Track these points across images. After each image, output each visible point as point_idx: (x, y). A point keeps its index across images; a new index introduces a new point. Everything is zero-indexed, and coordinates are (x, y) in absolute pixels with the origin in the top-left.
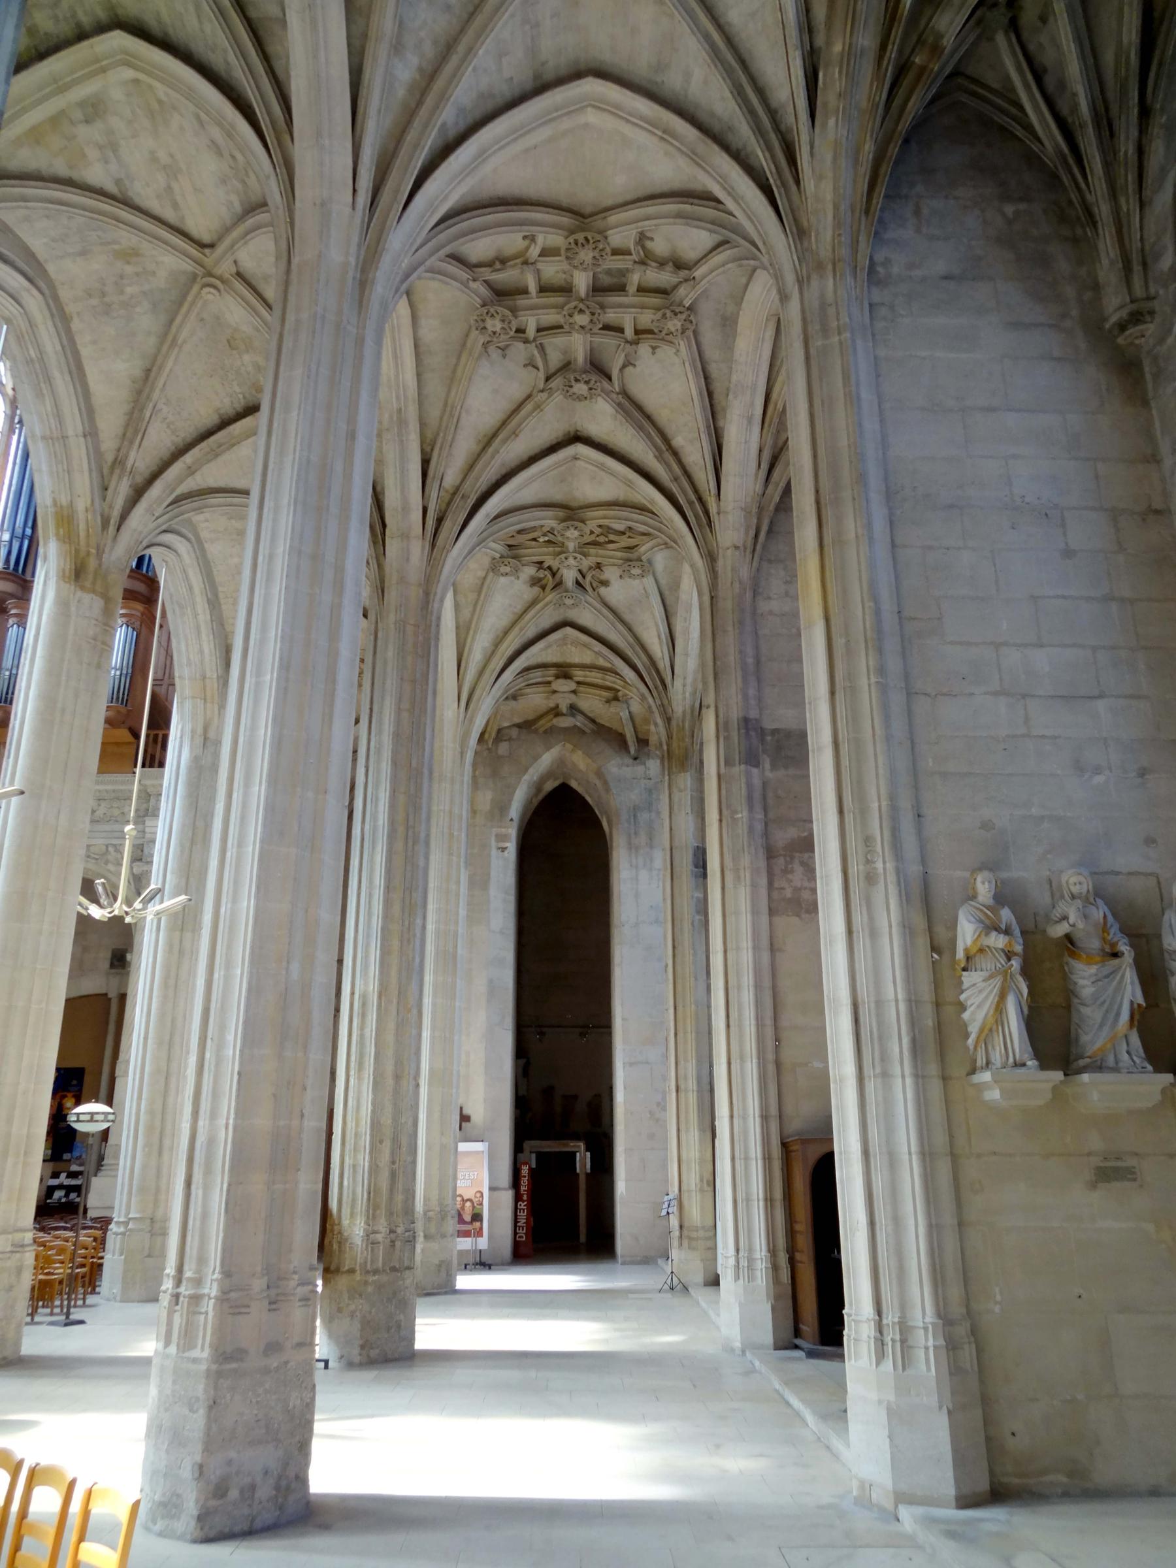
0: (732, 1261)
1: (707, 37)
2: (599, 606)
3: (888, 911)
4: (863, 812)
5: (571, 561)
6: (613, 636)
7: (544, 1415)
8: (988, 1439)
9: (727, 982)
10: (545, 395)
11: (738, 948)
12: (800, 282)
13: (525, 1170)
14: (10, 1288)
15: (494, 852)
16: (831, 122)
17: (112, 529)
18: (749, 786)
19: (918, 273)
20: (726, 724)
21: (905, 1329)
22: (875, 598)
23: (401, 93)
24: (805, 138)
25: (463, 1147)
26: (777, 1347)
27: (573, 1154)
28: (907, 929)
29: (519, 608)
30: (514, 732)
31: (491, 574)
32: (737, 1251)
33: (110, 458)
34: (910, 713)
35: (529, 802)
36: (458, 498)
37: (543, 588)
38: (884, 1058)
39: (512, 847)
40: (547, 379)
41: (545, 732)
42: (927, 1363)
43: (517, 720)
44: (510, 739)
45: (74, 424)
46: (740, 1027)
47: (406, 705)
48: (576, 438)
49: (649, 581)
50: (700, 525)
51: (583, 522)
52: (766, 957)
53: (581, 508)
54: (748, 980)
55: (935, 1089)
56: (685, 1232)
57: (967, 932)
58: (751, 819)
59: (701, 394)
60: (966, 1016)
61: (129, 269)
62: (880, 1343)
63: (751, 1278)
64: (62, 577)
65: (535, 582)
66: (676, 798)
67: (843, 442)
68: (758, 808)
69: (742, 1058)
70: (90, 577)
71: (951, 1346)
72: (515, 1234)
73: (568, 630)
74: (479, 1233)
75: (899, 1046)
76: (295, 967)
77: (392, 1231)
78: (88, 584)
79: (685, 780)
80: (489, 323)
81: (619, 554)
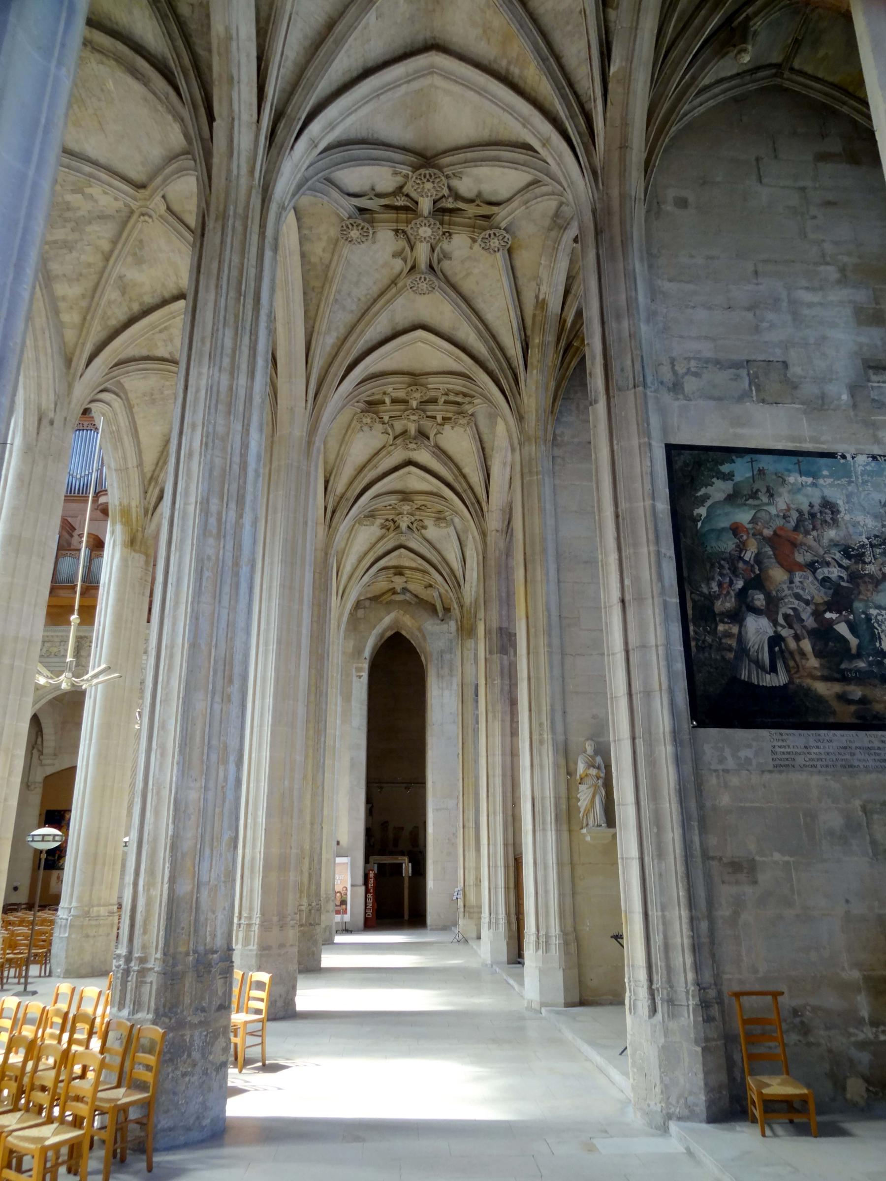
0: (487, 920)
1: (476, 327)
2: (420, 540)
3: (548, 756)
4: (539, 712)
5: (405, 519)
6: (428, 555)
7: (392, 988)
8: (580, 981)
9: (487, 772)
10: (393, 447)
11: (494, 755)
12: (520, 444)
13: (372, 874)
14: (108, 935)
15: (355, 679)
16: (535, 372)
17: (149, 515)
18: (501, 664)
19: (576, 440)
20: (490, 630)
21: (547, 936)
22: (548, 610)
23: (328, 349)
24: (523, 378)
26: (509, 963)
27: (400, 865)
28: (556, 765)
29: (374, 540)
30: (367, 603)
31: (357, 525)
32: (490, 914)
33: (148, 476)
34: (563, 664)
35: (376, 645)
36: (344, 500)
37: (388, 529)
38: (544, 822)
39: (365, 675)
40: (395, 438)
41: (387, 603)
42: (555, 950)
43: (369, 596)
44: (364, 608)
45: (132, 462)
46: (494, 797)
47: (315, 619)
48: (410, 463)
49: (451, 530)
50: (477, 516)
51: (413, 501)
52: (508, 759)
53: (411, 493)
54: (498, 771)
55: (565, 835)
56: (467, 909)
57: (581, 768)
58: (502, 684)
59: (478, 451)
60: (579, 804)
61: (168, 383)
62: (538, 943)
63: (497, 928)
64: (124, 545)
65: (383, 527)
66: (465, 655)
67: (537, 531)
68: (506, 677)
69: (495, 813)
70: (138, 544)
71: (566, 943)
72: (366, 913)
73: (402, 550)
74: (345, 912)
75: (550, 818)
76: (286, 783)
77: (310, 905)
78: (137, 548)
79: (470, 643)
80: (365, 420)
81: (433, 515)
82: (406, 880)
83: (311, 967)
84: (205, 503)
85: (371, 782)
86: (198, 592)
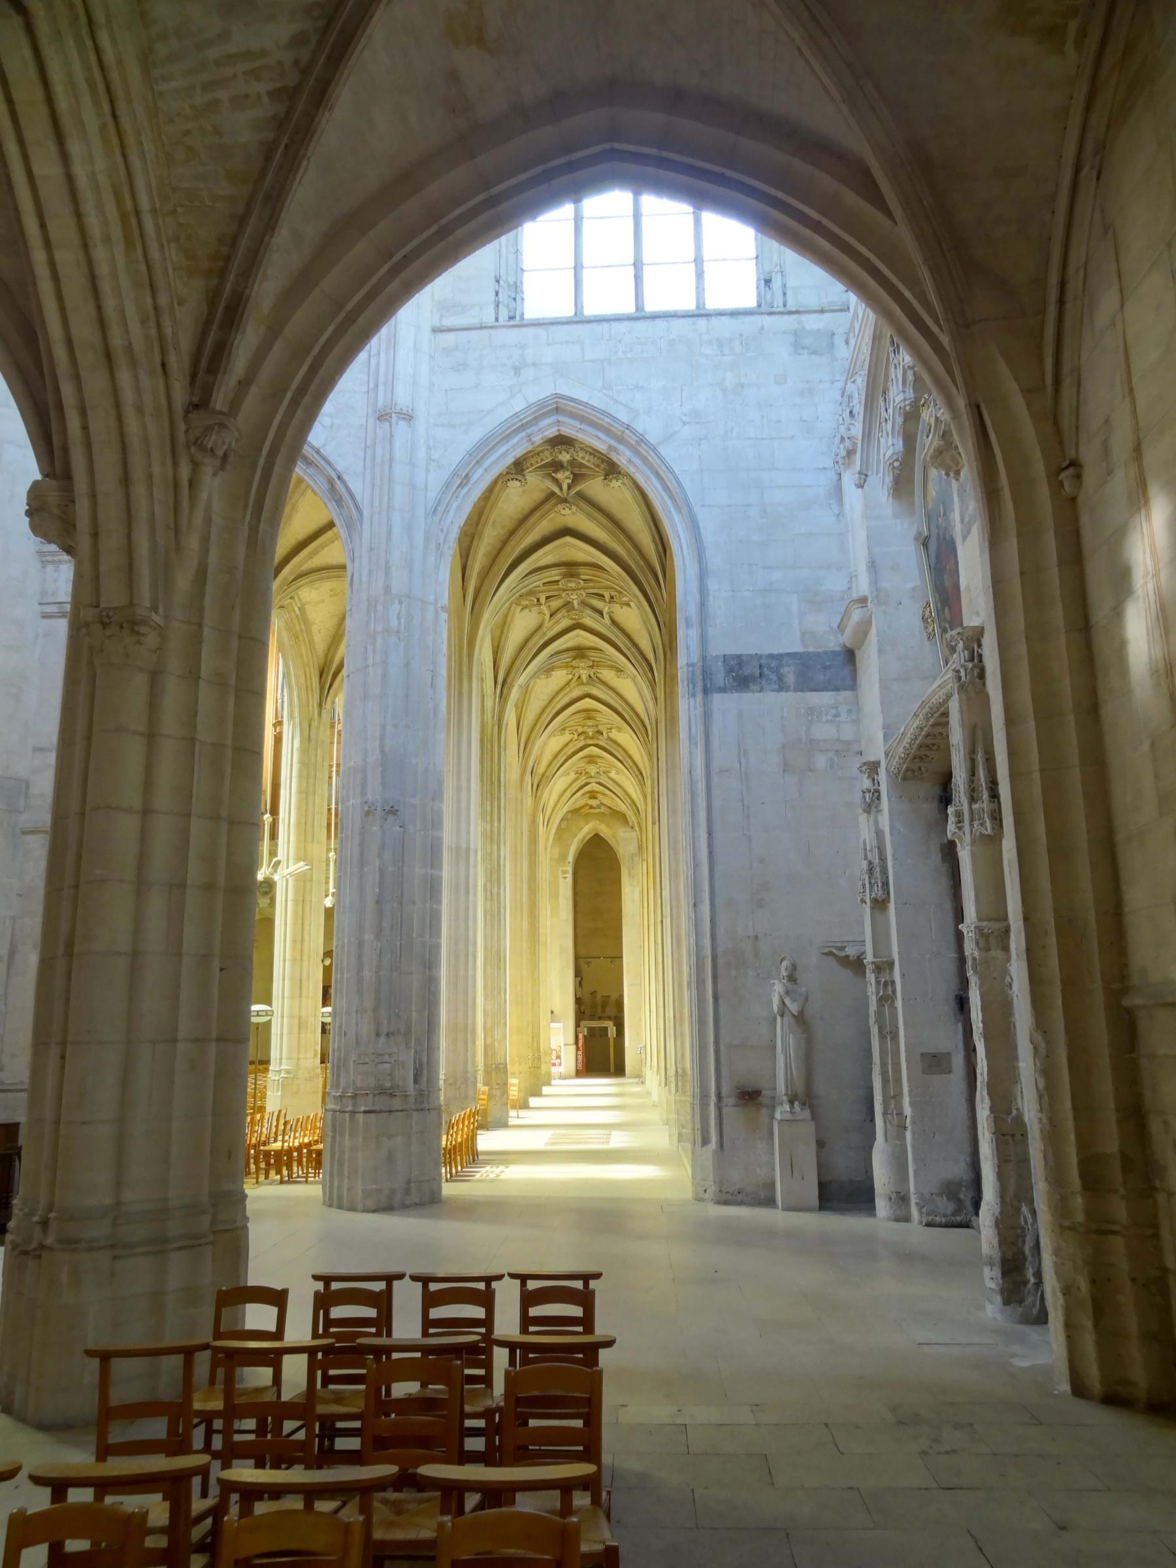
13: (581, 1036)
15: (561, 879)
25: (553, 1025)
30: (569, 816)
39: (570, 876)
82: (612, 1041)
83: (538, 1094)
84: (485, 885)
85: (577, 959)
86: (485, 925)
